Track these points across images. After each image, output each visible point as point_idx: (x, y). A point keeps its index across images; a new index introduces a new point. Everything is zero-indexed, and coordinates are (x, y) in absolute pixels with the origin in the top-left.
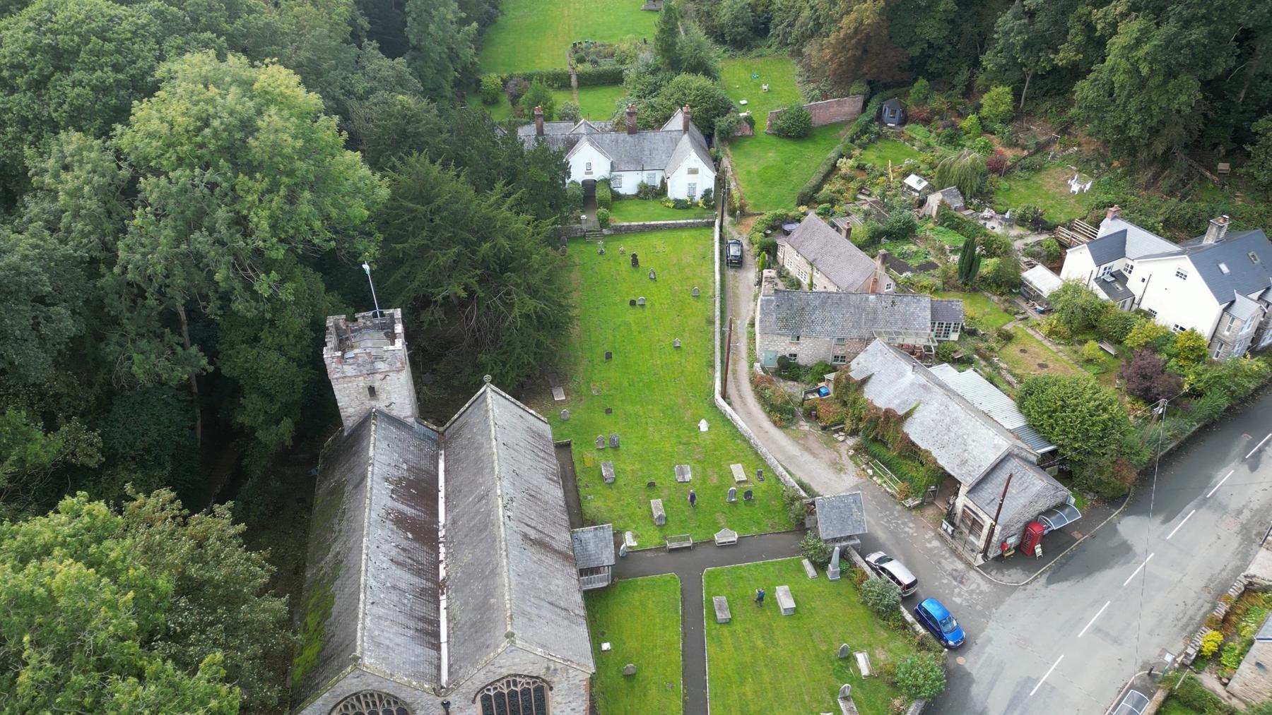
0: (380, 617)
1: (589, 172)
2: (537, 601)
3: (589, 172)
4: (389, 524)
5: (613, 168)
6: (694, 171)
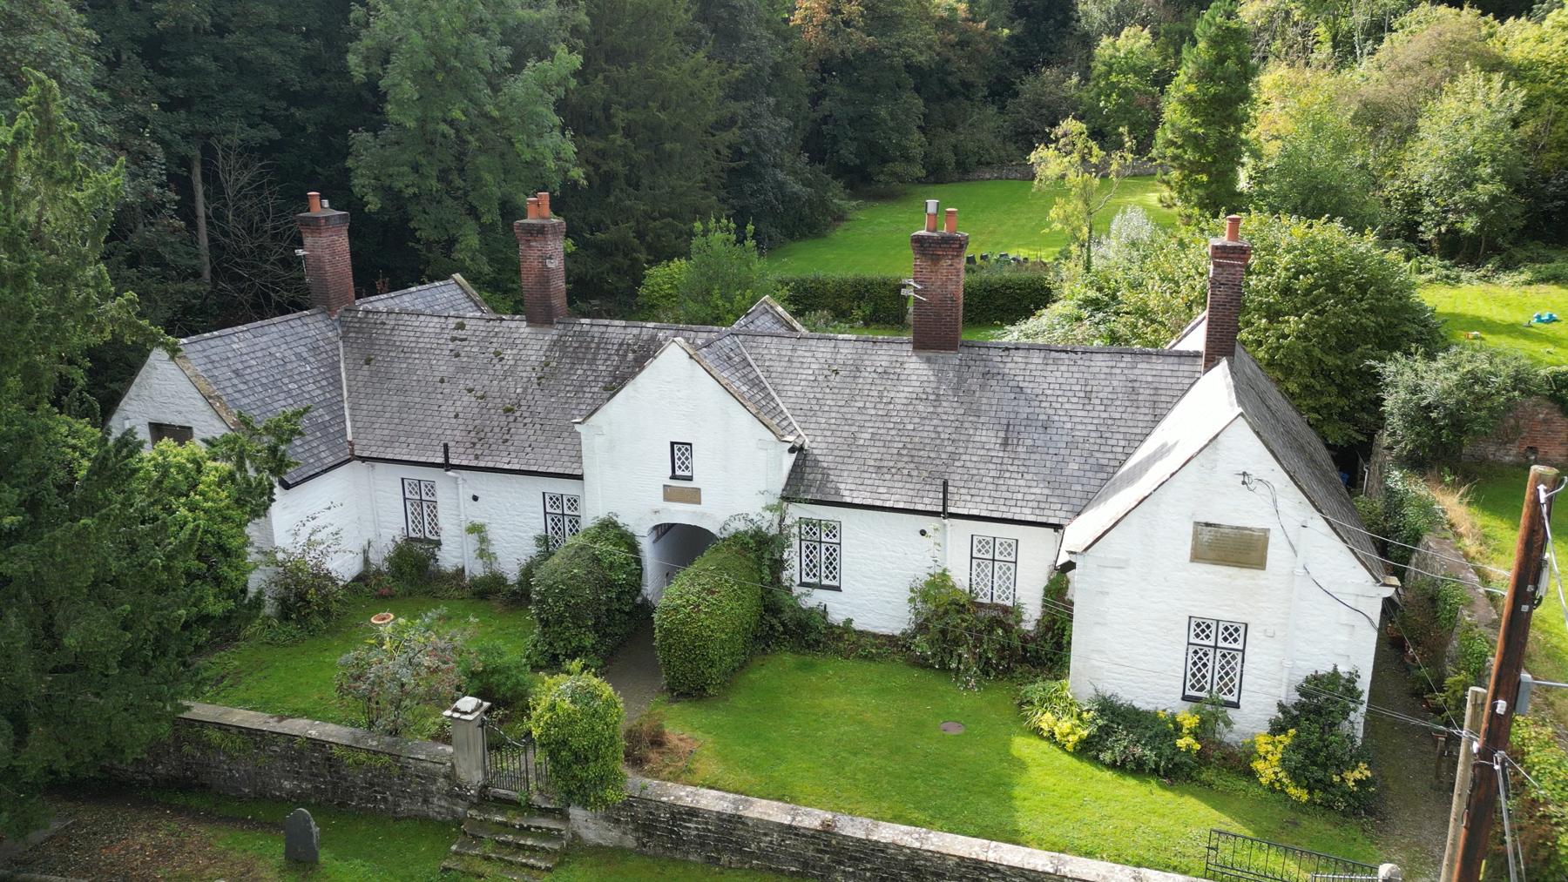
1: (681, 486)
3: (681, 486)
5: (803, 480)
6: (1234, 549)
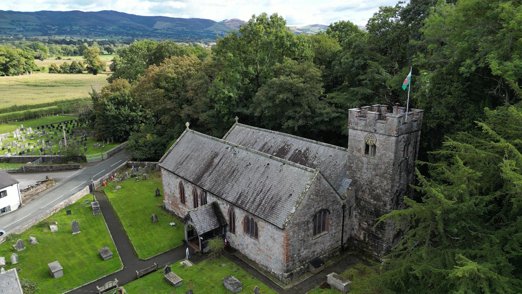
0: (248, 134)
2: (192, 149)
4: (283, 145)
